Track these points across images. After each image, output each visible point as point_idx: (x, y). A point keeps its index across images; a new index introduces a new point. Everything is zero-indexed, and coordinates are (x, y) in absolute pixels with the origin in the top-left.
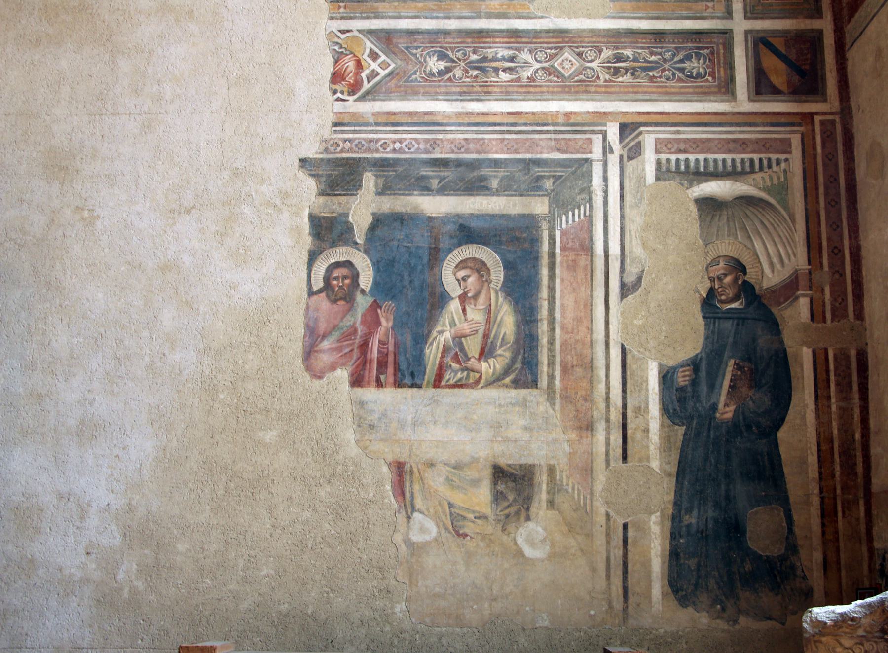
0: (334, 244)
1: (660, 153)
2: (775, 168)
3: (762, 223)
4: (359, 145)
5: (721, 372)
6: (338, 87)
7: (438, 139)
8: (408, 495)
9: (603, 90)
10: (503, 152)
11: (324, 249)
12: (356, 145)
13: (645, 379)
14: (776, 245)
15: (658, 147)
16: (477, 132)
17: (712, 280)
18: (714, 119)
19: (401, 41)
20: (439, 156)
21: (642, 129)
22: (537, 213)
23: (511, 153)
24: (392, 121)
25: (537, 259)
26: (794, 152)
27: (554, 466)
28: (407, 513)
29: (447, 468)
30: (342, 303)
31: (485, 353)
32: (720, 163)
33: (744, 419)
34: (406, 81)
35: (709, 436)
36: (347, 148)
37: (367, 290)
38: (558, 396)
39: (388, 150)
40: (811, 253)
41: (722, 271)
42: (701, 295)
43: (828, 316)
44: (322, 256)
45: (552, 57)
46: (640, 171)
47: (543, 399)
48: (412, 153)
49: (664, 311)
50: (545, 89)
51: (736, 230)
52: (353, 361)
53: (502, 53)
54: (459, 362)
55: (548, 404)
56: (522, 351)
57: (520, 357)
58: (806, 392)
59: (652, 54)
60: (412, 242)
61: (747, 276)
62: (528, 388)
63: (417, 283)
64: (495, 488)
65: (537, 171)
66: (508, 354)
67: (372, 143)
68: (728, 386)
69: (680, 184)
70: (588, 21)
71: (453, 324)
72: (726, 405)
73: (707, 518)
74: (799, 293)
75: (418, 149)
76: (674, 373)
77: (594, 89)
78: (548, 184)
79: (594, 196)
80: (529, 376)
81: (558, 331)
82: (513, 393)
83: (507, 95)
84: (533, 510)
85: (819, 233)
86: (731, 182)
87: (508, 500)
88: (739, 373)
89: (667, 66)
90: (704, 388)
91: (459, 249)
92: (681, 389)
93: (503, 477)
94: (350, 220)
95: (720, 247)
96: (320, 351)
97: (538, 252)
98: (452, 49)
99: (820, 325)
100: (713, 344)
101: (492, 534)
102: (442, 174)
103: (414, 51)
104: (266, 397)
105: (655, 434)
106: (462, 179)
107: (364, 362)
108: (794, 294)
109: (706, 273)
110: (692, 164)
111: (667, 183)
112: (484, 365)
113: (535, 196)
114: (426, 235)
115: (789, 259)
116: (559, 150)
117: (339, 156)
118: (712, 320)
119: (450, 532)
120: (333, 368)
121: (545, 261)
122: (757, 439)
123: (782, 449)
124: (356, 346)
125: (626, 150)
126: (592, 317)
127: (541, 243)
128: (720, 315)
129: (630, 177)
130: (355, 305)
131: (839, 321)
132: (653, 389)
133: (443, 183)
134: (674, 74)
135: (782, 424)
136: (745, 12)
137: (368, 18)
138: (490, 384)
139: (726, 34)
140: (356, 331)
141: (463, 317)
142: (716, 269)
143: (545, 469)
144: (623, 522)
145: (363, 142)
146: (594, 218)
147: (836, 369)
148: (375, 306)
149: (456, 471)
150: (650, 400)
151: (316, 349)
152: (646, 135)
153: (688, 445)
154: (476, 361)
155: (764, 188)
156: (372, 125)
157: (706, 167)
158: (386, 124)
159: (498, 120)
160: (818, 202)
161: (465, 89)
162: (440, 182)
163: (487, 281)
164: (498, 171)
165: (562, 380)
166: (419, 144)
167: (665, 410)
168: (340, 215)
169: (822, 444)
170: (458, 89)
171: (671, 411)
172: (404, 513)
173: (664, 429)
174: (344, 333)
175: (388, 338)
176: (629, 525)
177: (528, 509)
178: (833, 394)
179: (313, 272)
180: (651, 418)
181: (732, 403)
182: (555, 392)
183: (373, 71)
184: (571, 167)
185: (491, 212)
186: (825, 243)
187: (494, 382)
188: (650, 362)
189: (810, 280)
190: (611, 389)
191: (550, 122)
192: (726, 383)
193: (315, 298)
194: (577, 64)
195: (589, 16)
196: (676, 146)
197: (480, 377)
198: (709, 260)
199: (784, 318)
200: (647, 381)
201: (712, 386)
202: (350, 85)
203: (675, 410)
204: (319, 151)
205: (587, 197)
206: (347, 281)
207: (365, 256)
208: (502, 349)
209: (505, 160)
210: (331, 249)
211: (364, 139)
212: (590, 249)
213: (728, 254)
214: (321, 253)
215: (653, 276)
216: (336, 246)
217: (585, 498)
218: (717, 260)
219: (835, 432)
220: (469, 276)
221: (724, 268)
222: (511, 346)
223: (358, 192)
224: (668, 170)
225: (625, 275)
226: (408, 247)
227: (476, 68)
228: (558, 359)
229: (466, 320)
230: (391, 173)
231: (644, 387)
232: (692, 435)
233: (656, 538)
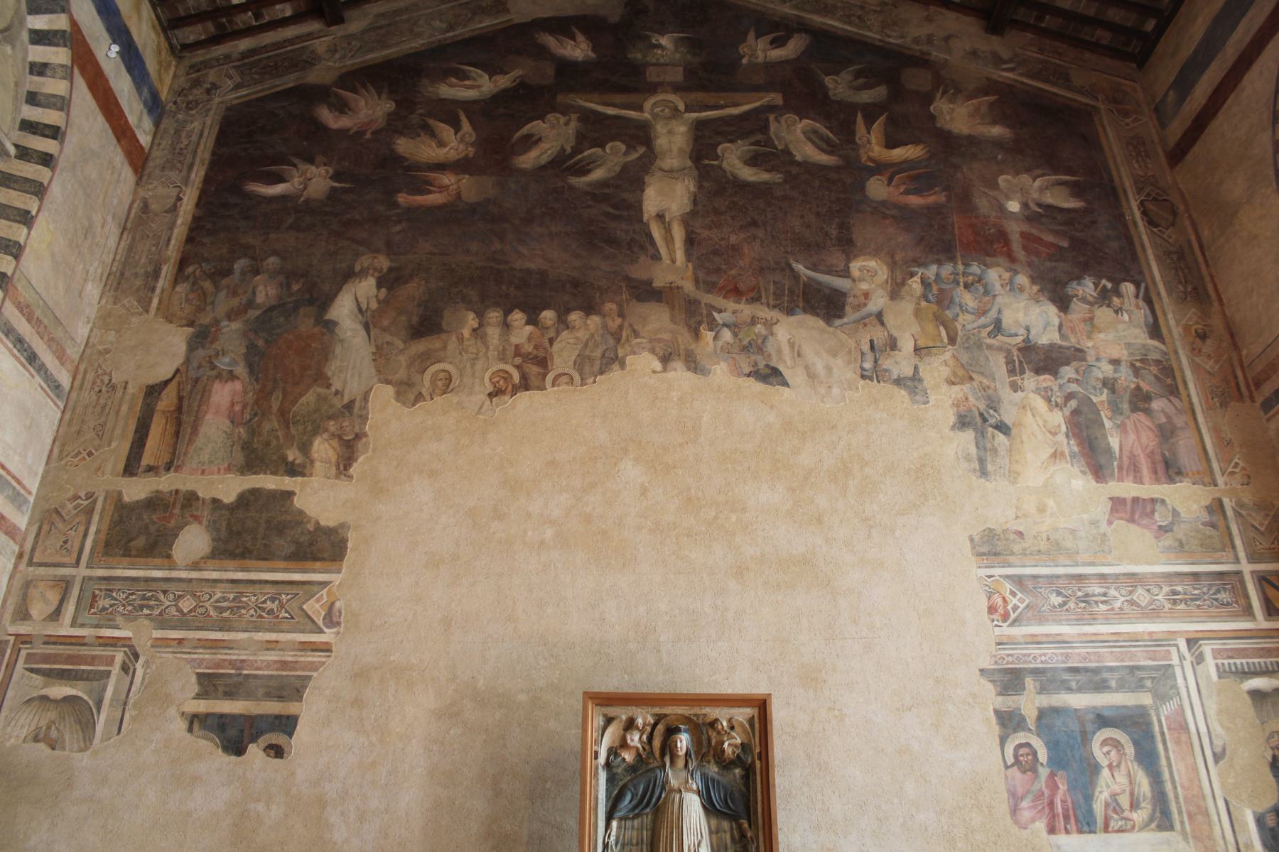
0: (1015, 731)
6: (994, 617)
9: (1168, 615)
10: (1114, 662)
18: (1244, 634)
19: (1029, 583)
21: (1201, 642)
24: (1035, 641)
25: (1153, 737)
30: (1029, 773)
31: (1134, 805)
32: (1257, 665)
34: (1039, 612)
37: (1045, 763)
44: (1009, 740)
45: (1131, 592)
47: (1180, 838)
50: (1131, 616)
53: (1098, 590)
54: (1117, 813)
57: (1158, 809)
59: (1195, 589)
60: (1067, 727)
63: (1077, 757)
66: (1149, 807)
70: (1149, 567)
71: (1108, 786)
75: (1057, 660)
77: (1162, 615)
78: (1148, 683)
79: (1180, 691)
80: (1167, 823)
81: (1179, 789)
83: (1107, 620)
89: (1206, 597)
91: (1100, 732)
94: (1023, 712)
96: (1023, 809)
97: (1152, 732)
98: (1065, 588)
102: (1077, 678)
103: (1039, 590)
104: (990, 844)
106: (1091, 681)
107: (1053, 817)
110: (1239, 666)
116: (1150, 659)
120: (1033, 820)
121: (1158, 738)
124: (1045, 805)
134: (1212, 603)
136: (1248, 559)
137: (1003, 567)
139: (1239, 573)
140: (1043, 794)
148: (1052, 775)
156: (1022, 644)
157: (1249, 668)
158: (1032, 643)
161: (1079, 617)
162: (1077, 683)
165: (1190, 824)
168: (1015, 709)
170: (1074, 617)
182: (1187, 833)
183: (1015, 604)
185: (1115, 704)
194: (1148, 598)
195: (1148, 563)
202: (1002, 615)
205: (1176, 692)
206: (1030, 757)
211: (1022, 654)
212: (1184, 727)
220: (1110, 751)
224: (1225, 671)
227: (1083, 602)
228: (1184, 810)
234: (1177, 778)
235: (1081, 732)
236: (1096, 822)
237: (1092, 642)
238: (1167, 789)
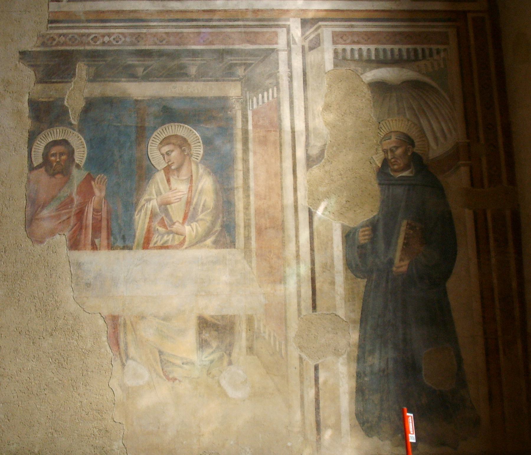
0: (51, 125)
1: (337, 44)
2: (436, 57)
4: (73, 39)
7: (142, 33)
8: (122, 345)
11: (43, 130)
12: (70, 39)
14: (439, 123)
15: (335, 39)
16: (176, 27)
17: (385, 151)
20: (143, 48)
21: (320, 23)
22: (231, 95)
23: (207, 45)
27: (252, 316)
28: (122, 362)
29: (157, 320)
30: (59, 176)
32: (389, 53)
36: (62, 42)
37: (82, 165)
38: (254, 254)
39: (98, 43)
41: (394, 145)
42: (376, 164)
43: (486, 181)
44: (41, 136)
48: (119, 45)
52: (70, 227)
54: (165, 226)
55: (245, 262)
56: (221, 216)
57: (220, 221)
62: (228, 248)
64: (200, 337)
65: (229, 59)
66: (209, 218)
67: (84, 37)
71: (159, 193)
72: (401, 260)
73: (388, 359)
75: (125, 41)
76: (355, 233)
81: (252, 198)
82: (215, 252)
84: (234, 355)
87: (212, 347)
88: (412, 232)
90: (381, 245)
91: (163, 127)
92: (362, 247)
93: (207, 327)
94: (66, 103)
95: (391, 124)
101: (198, 378)
102: (146, 63)
107: (80, 227)
110: (365, 53)
112: (187, 229)
113: (229, 81)
114: (133, 116)
117: (54, 48)
119: (160, 377)
120: (52, 233)
123: (451, 297)
124: (73, 214)
126: (281, 185)
127: (235, 121)
128: (393, 182)
130: (71, 178)
133: (147, 71)
138: (193, 246)
140: (72, 201)
141: (168, 187)
143: (244, 319)
144: (314, 364)
145: (76, 36)
146: (281, 100)
148: (89, 179)
149: (165, 323)
151: (37, 217)
152: (324, 29)
154: (180, 225)
157: (377, 56)
158: (96, 21)
159: (194, 16)
162: (144, 70)
163: (188, 155)
164: (196, 60)
165: (257, 240)
166: (125, 37)
167: (349, 265)
172: (119, 361)
174: (62, 203)
175: (102, 206)
176: (320, 367)
177: (230, 355)
179: (33, 150)
182: (251, 251)
184: (260, 56)
185: (190, 95)
187: (197, 243)
190: (301, 247)
191: (240, 18)
192: (401, 241)
193: (35, 172)
197: (184, 239)
198: (382, 135)
201: (388, 244)
203: (357, 265)
204: (37, 45)
206: (64, 157)
207: (79, 135)
208: (203, 214)
209: (202, 50)
210: (48, 130)
211: (77, 34)
213: (399, 130)
214: (39, 133)
215: (335, 149)
216: (53, 127)
217: (280, 344)
219: (495, 281)
220: (172, 151)
222: (211, 211)
223: (73, 79)
224: (344, 59)
225: (310, 149)
226: (118, 127)
228: (253, 222)
229: (170, 189)
230: (101, 63)
232: (373, 287)
233: (343, 377)
234: (252, 184)
235: (137, 127)
236: (135, 236)
237: (177, 20)
238: (236, 198)
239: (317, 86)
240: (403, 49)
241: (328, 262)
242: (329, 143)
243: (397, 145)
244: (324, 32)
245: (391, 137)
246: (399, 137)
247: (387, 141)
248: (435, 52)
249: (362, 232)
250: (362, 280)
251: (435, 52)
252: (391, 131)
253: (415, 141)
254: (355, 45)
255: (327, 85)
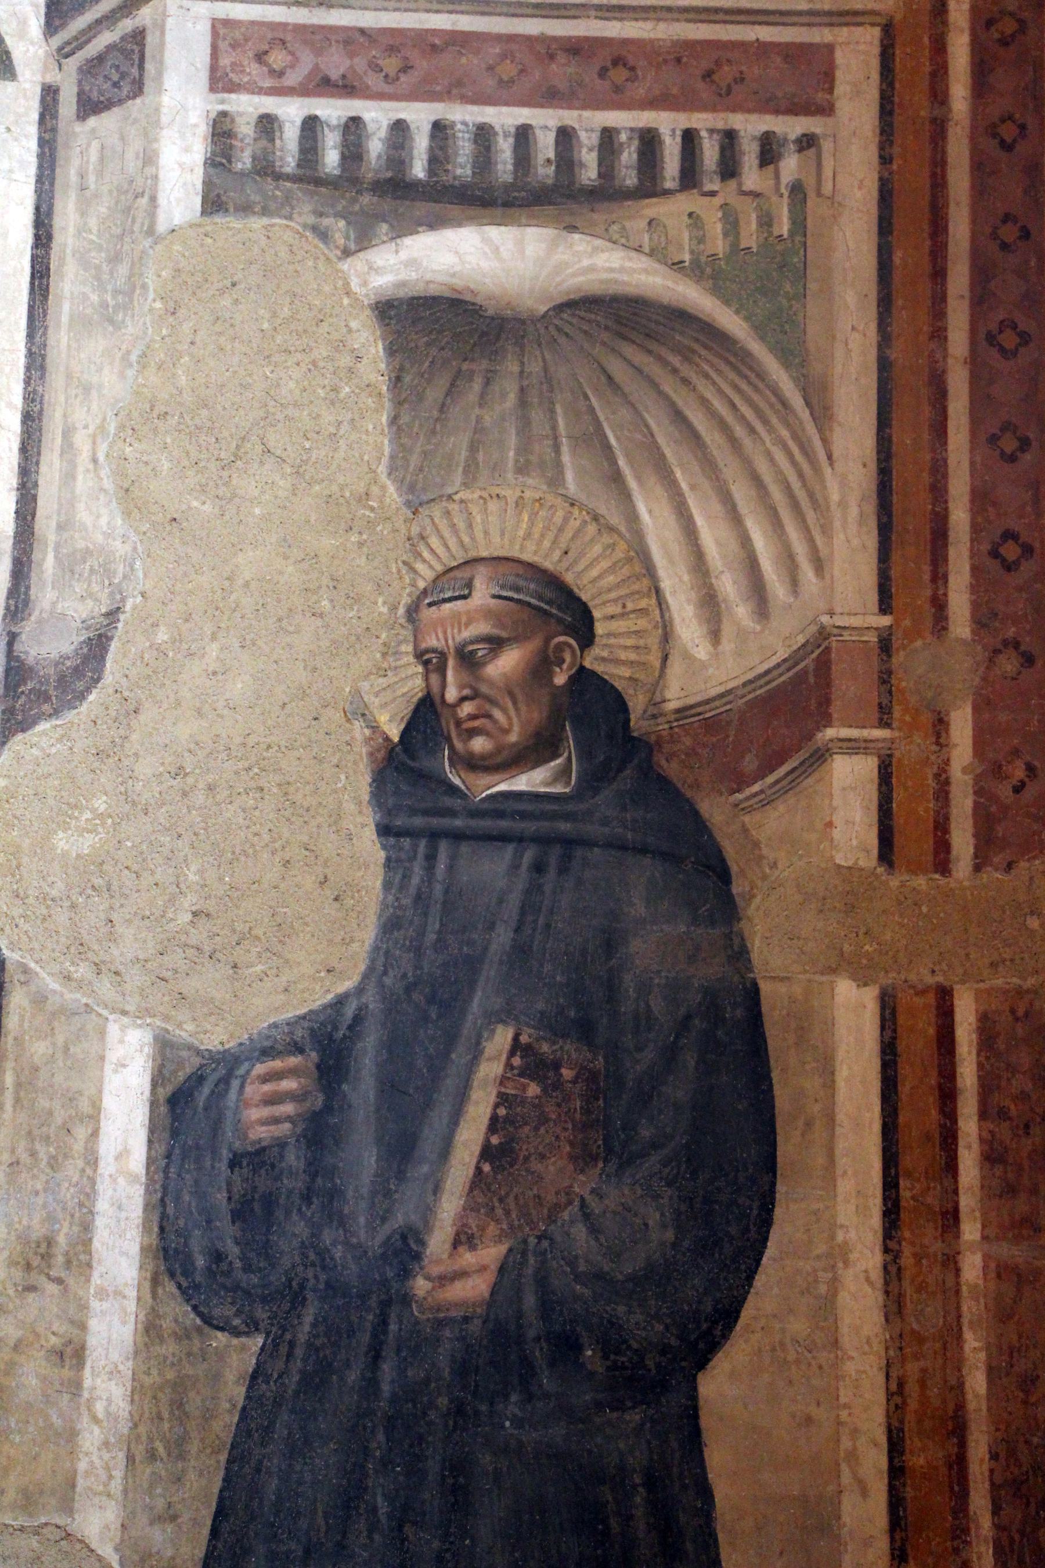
1: (232, 88)
2: (752, 177)
3: (679, 417)
5: (450, 1083)
13: (85, 1106)
14: (736, 519)
15: (225, 61)
26: (844, 107)
32: (505, 149)
33: (546, 1308)
35: (370, 1385)
40: (895, 556)
41: (483, 628)
42: (375, 728)
46: (132, 165)
49: (200, 798)
51: (557, 448)
58: (845, 1186)
61: (596, 651)
68: (477, 1149)
69: (314, 229)
72: (463, 1239)
74: (830, 733)
76: (225, 1081)
85: (939, 470)
86: (548, 233)
88: (533, 1090)
99: (920, 882)
100: (418, 951)
105: (114, 1373)
108: (810, 737)
109: (407, 633)
110: (375, 147)
111: (257, 223)
115: (794, 583)
118: (423, 844)
122: (599, 1406)
125: (72, 64)
128: (458, 823)
129: (83, 189)
131: (1009, 866)
132: (122, 1155)
135: (725, 1337)
142: (456, 616)
147: (987, 1087)
150: (102, 1205)
153: (268, 1430)
155: (696, 263)
157: (437, 160)
160: (939, 334)
169: (912, 1441)
171: (200, 1262)
173: (162, 1350)
178: (967, 1201)
180: (102, 1294)
181: (492, 1229)
186: (960, 516)
188: (113, 1030)
189: (885, 678)
196: (307, 61)
198: (426, 573)
199: (756, 844)
200: (94, 1117)
203: (218, 1257)
213: (515, 553)
215: (162, 635)
218: (464, 574)
221: (488, 614)
225: (27, 629)
231: (78, 1147)
239: (104, 305)
240: (583, 135)
241: (62, 1239)
242: (135, 607)
243: (496, 632)
244: (170, 22)
245: (469, 585)
246: (517, 589)
247: (448, 606)
248: (750, 154)
249: (265, 1079)
250: (235, 1341)
251: (750, 154)
252: (473, 554)
253: (597, 614)
254: (323, 101)
255: (158, 305)
